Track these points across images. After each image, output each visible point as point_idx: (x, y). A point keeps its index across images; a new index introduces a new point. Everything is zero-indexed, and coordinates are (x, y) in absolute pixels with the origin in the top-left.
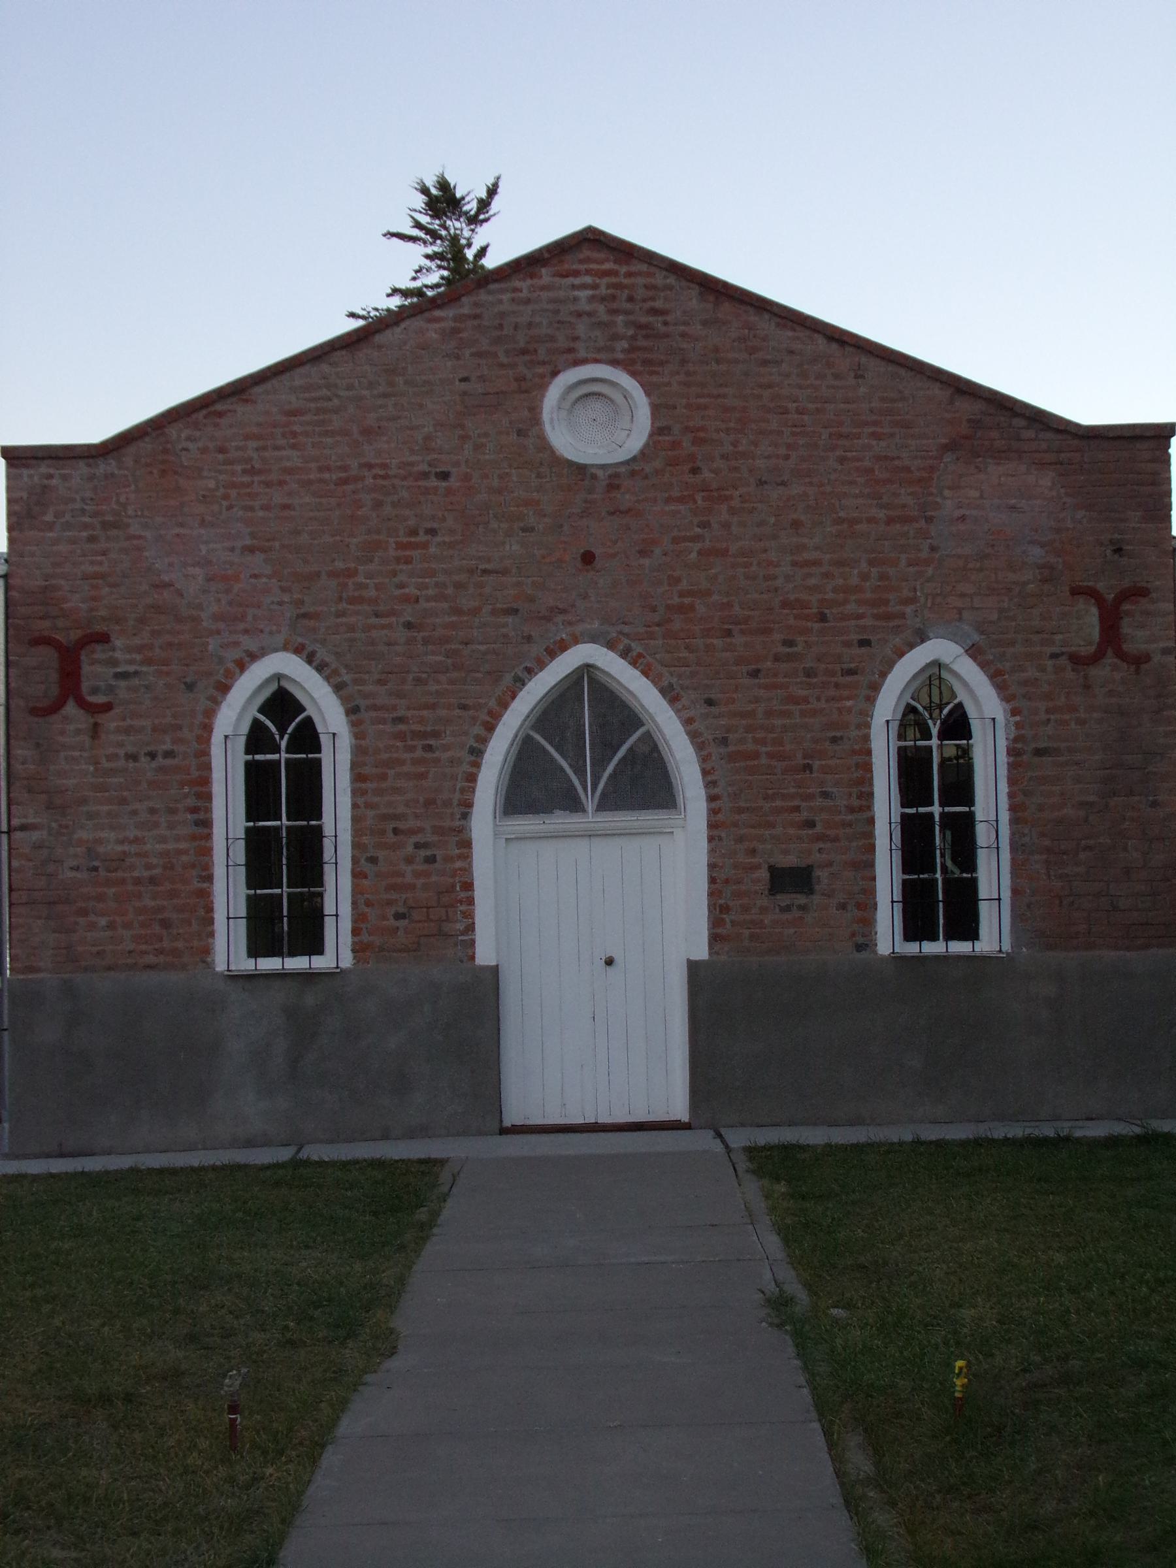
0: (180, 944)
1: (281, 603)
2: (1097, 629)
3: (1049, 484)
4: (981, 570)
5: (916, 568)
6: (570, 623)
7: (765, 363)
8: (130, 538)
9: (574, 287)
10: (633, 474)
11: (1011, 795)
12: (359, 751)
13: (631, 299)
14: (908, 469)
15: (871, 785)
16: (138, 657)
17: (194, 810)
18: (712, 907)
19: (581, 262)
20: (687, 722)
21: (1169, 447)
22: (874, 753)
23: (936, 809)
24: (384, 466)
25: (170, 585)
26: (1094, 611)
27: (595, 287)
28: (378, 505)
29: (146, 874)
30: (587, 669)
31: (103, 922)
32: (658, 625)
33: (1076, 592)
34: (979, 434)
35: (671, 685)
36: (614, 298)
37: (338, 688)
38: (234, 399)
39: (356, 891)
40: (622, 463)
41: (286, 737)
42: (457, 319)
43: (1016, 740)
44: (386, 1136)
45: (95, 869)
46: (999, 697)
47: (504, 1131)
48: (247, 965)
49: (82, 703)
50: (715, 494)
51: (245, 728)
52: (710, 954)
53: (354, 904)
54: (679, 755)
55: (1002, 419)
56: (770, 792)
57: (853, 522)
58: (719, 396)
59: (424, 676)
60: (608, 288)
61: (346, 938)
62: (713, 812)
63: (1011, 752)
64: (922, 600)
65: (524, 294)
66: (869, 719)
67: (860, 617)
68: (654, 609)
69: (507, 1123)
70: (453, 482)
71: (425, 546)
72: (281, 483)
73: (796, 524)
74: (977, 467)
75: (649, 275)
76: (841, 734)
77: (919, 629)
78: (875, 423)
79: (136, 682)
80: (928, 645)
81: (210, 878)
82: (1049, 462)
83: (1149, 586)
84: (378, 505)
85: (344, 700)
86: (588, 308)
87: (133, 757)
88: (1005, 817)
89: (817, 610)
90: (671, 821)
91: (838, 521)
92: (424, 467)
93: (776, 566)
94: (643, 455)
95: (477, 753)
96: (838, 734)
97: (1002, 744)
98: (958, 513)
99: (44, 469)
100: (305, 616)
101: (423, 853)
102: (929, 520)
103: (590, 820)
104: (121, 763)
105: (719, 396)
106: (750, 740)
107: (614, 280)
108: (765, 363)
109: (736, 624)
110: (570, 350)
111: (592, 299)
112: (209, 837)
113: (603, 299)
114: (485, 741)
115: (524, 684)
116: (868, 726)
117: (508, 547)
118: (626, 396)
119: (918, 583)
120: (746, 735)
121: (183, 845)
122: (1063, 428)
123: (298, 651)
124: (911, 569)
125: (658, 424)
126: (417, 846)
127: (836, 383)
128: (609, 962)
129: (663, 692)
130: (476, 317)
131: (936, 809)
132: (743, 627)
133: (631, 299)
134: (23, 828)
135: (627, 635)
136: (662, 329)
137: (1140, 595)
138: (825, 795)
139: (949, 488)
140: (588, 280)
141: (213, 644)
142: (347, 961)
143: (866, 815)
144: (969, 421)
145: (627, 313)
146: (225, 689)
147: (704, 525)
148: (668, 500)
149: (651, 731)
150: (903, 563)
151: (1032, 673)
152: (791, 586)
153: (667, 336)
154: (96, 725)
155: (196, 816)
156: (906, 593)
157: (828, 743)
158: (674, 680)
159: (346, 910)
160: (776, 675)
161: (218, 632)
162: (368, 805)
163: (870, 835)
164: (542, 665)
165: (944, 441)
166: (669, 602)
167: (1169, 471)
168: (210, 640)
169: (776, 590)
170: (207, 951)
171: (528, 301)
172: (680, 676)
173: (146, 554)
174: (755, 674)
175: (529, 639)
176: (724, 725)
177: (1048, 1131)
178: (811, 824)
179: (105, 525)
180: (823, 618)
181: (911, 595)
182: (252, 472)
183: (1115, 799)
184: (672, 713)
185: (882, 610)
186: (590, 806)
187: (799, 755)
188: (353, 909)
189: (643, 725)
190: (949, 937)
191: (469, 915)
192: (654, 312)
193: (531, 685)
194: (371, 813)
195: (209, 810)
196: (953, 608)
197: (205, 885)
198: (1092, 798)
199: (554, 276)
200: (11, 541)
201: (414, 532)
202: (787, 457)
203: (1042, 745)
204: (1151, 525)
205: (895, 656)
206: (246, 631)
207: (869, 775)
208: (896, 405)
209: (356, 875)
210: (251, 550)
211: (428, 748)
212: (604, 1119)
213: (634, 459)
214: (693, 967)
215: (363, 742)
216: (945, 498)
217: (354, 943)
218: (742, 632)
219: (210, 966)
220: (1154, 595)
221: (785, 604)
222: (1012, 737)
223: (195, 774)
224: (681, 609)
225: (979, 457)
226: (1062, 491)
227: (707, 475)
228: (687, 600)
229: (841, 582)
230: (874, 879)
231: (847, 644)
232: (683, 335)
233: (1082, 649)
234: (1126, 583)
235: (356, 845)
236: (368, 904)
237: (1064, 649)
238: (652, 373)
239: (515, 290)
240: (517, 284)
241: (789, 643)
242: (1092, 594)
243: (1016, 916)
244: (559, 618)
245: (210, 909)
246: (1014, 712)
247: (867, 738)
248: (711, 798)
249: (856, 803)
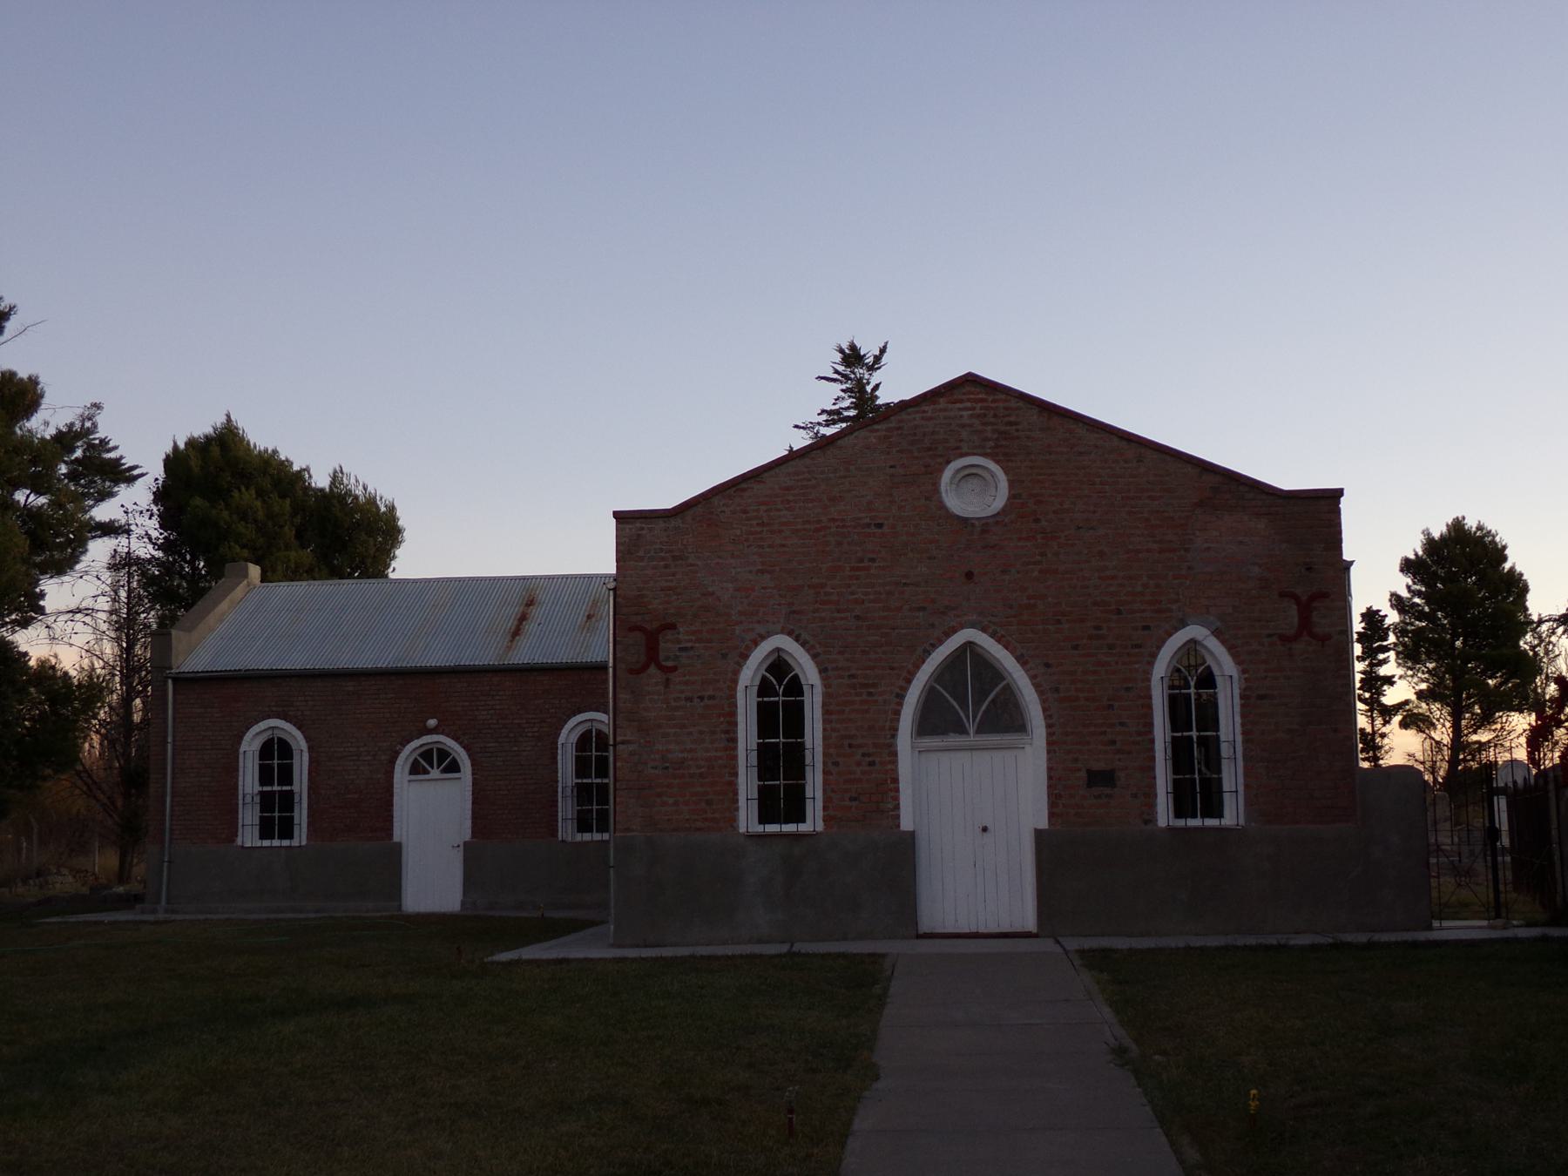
0: (717, 815)
1: (779, 605)
6: (958, 616)
7: (1081, 453)
8: (692, 565)
9: (960, 409)
10: (997, 523)
11: (1243, 725)
12: (827, 696)
13: (995, 416)
15: (1152, 718)
16: (694, 638)
17: (727, 732)
18: (1049, 795)
19: (964, 394)
20: (1033, 678)
23: (1194, 734)
24: (843, 520)
25: (712, 594)
27: (974, 409)
28: (839, 544)
29: (698, 771)
30: (969, 645)
31: (671, 801)
32: (1015, 616)
33: (1283, 595)
36: (985, 415)
37: (814, 657)
38: (752, 481)
39: (825, 783)
40: (991, 516)
41: (782, 687)
42: (888, 430)
43: (1245, 689)
44: (845, 938)
45: (667, 768)
47: (919, 937)
48: (760, 829)
49: (660, 667)
51: (757, 682)
52: (1049, 826)
53: (824, 791)
54: (1027, 699)
58: (1051, 475)
59: (867, 649)
60: (981, 409)
61: (820, 813)
62: (1049, 735)
63: (1242, 697)
65: (929, 414)
67: (1144, 611)
69: (921, 931)
70: (885, 529)
71: (867, 569)
72: (780, 531)
73: (1101, 554)
75: (1006, 401)
79: (692, 653)
81: (736, 775)
84: (839, 544)
85: (818, 664)
86: (968, 422)
87: (690, 699)
88: (1239, 739)
92: (868, 520)
94: (1004, 511)
95: (901, 697)
96: (1130, 685)
97: (1237, 692)
98: (1206, 545)
99: (638, 525)
100: (794, 612)
101: (868, 759)
102: (1187, 550)
103: (972, 739)
104: (683, 703)
105: (1051, 475)
107: (985, 404)
108: (1081, 453)
110: (958, 448)
111: (971, 416)
112: (735, 748)
113: (978, 416)
114: (905, 689)
115: (930, 654)
116: (1149, 680)
117: (919, 569)
118: (993, 475)
121: (719, 754)
123: (790, 634)
124: (1176, 581)
125: (1013, 492)
126: (864, 755)
127: (1126, 465)
128: (985, 829)
130: (899, 428)
133: (995, 416)
134: (623, 743)
135: (994, 623)
136: (1016, 434)
138: (1122, 724)
140: (969, 405)
141: (738, 629)
142: (820, 827)
145: (992, 424)
146: (745, 657)
147: (1043, 554)
148: (1020, 539)
153: (1018, 438)
154: (668, 680)
155: (727, 736)
159: (819, 795)
161: (741, 622)
162: (833, 730)
163: (1152, 750)
164: (941, 642)
167: (1340, 518)
168: (737, 627)
170: (732, 821)
171: (931, 419)
173: (699, 575)
174: (1076, 647)
175: (933, 625)
177: (1272, 940)
178: (1113, 742)
179: (675, 558)
180: (1119, 612)
182: (762, 525)
184: (1023, 672)
186: (971, 732)
188: (824, 794)
189: (1004, 679)
190: (1203, 816)
191: (897, 799)
192: (1010, 424)
193: (934, 655)
194: (834, 735)
195: (735, 732)
197: (733, 779)
199: (948, 403)
200: (618, 568)
201: (861, 560)
202: (1094, 512)
206: (759, 622)
209: (825, 773)
210: (762, 572)
211: (870, 694)
212: (982, 930)
213: (998, 513)
214: (1039, 834)
215: (829, 690)
217: (824, 816)
219: (735, 828)
222: (1243, 686)
223: (727, 709)
227: (1044, 523)
228: (1032, 601)
229: (1130, 589)
230: (1155, 778)
232: (1028, 438)
235: (825, 755)
236: (833, 791)
238: (1008, 461)
239: (924, 412)
240: (926, 408)
241: (1098, 628)
243: (1248, 803)
245: (736, 793)
246: (1244, 671)
247: (1149, 688)
248: (1048, 726)
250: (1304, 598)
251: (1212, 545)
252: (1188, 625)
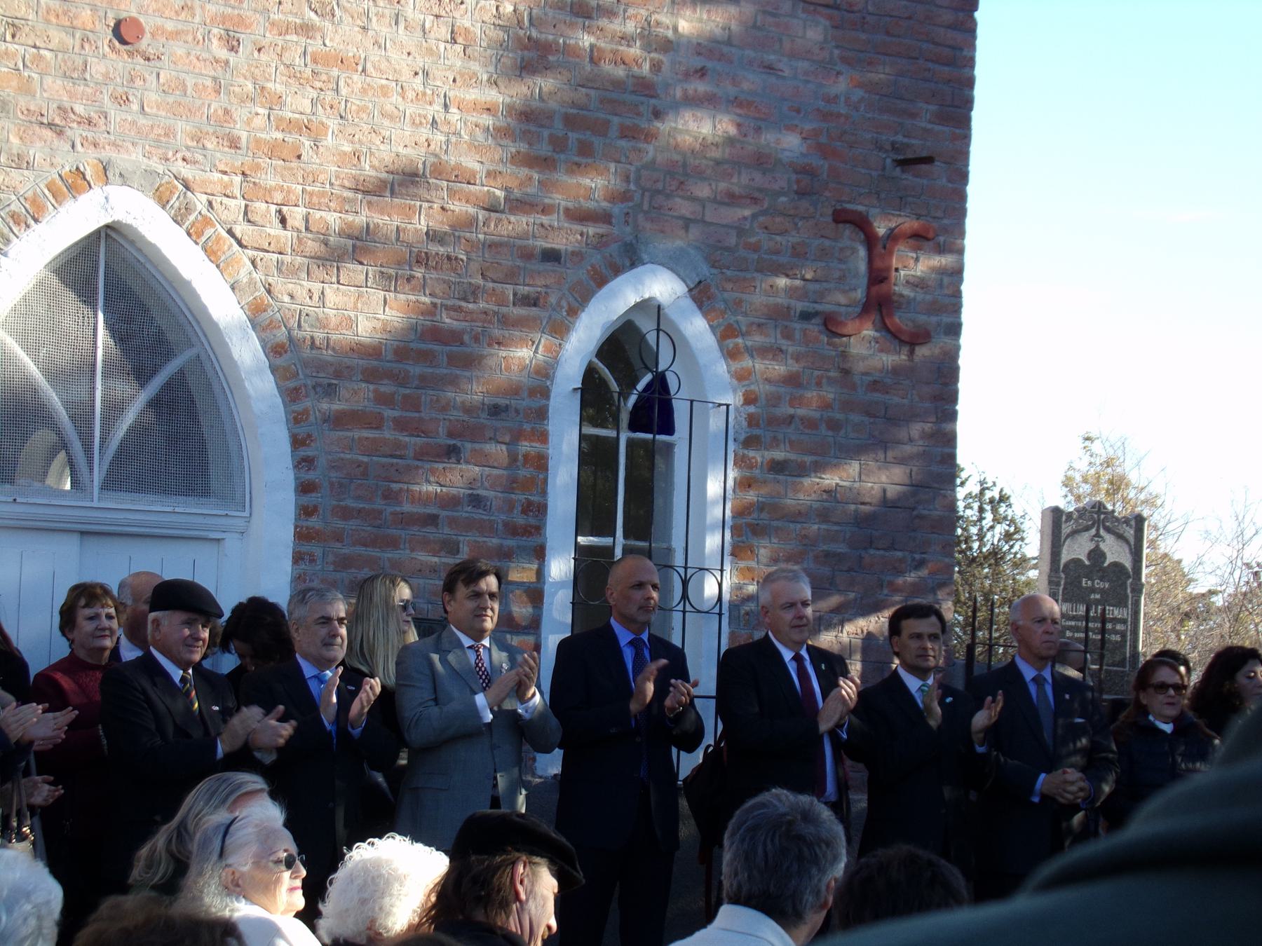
15: (544, 493)
33: (842, 218)
62: (305, 511)
64: (637, 197)
66: (548, 383)
68: (234, 144)
77: (631, 244)
103: (95, 504)
143: (533, 541)
149: (203, 357)
157: (484, 415)
167: (972, 47)
175: (21, 162)
183: (872, 552)
187: (442, 431)
198: (841, 548)
204: (946, 129)
207: (541, 476)
222: (742, 437)
226: (836, 52)
237: (819, 307)
244: (76, 132)
248: (304, 488)
249: (520, 520)
252: (644, 264)
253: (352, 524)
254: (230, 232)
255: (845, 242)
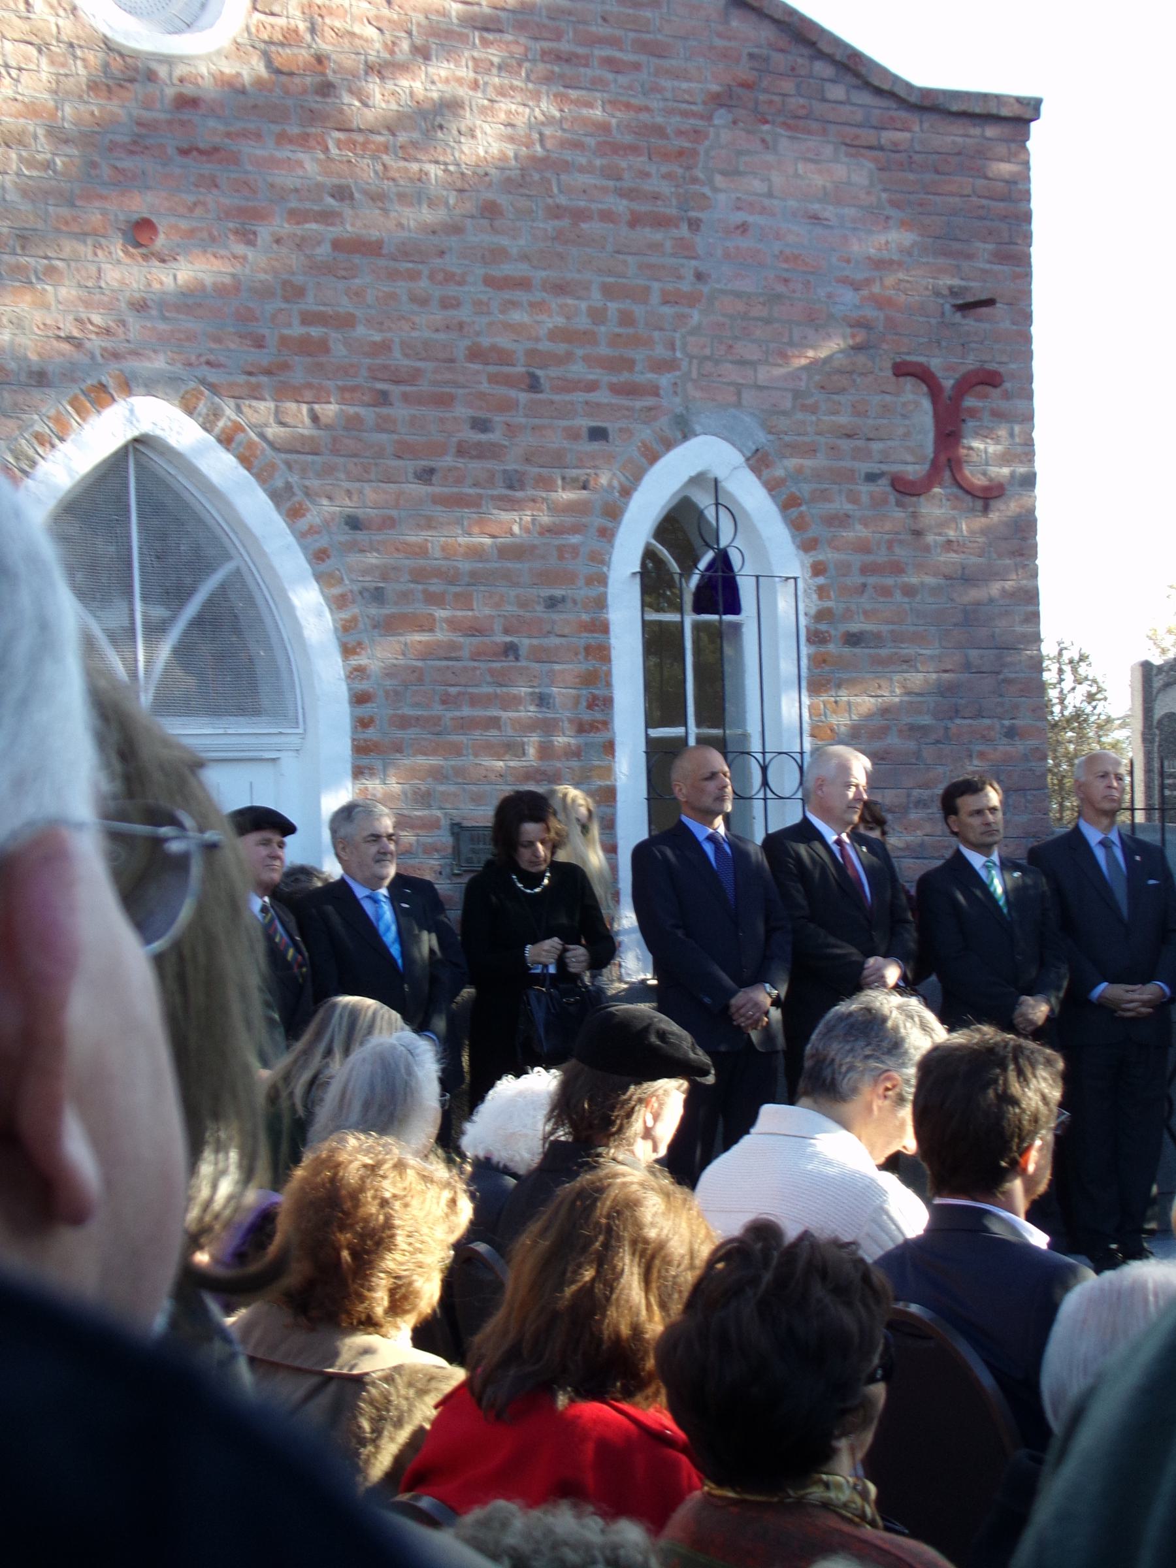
2: (931, 436)
3: (866, 182)
4: (768, 321)
5: (677, 309)
14: (660, 131)
15: (609, 685)
21: (1028, 139)
22: (615, 629)
26: (926, 404)
32: (268, 372)
33: (902, 370)
34: (765, 84)
35: (289, 487)
43: (821, 615)
46: (794, 542)
50: (360, 138)
55: (800, 61)
56: (453, 690)
57: (579, 215)
62: (362, 723)
64: (684, 365)
66: (605, 569)
67: (592, 387)
68: (259, 343)
74: (763, 141)
76: (563, 593)
77: (682, 416)
78: (614, 42)
80: (693, 444)
82: (865, 144)
83: (1002, 369)
89: (523, 369)
90: (282, 739)
91: (556, 212)
93: (460, 284)
96: (558, 592)
106: (421, 596)
109: (397, 382)
116: (603, 580)
119: (677, 335)
120: (412, 586)
122: (886, 87)
124: (667, 310)
129: (276, 496)
131: (693, 729)
132: (408, 389)
137: (987, 384)
139: (724, 173)
143: (598, 738)
144: (751, 56)
149: (244, 570)
150: (655, 298)
151: (841, 505)
152: (485, 320)
156: (660, 351)
157: (540, 608)
158: (294, 479)
160: (459, 481)
165: (715, 88)
166: (286, 332)
169: (461, 326)
172: (304, 471)
174: (426, 475)
176: (377, 567)
180: (534, 385)
181: (666, 354)
183: (958, 721)
184: (291, 539)
185: (625, 377)
187: (498, 627)
189: (228, 557)
196: (729, 384)
198: (926, 720)
203: (854, 627)
204: (1005, 268)
205: (644, 460)
207: (604, 668)
208: (641, 13)
216: (715, 190)
218: (406, 397)
220: (1008, 385)
221: (476, 354)
222: (813, 611)
224: (306, 346)
225: (766, 122)
226: (884, 196)
228: (315, 332)
229: (560, 321)
231: (573, 434)
233: (910, 468)
234: (971, 363)
237: (884, 467)
241: (481, 425)
242: (924, 376)
246: (818, 569)
247: (601, 603)
249: (587, 716)
250: (948, 384)
251: (751, 219)
252: (696, 435)
253: (411, 733)
254: (262, 436)
255: (908, 396)
